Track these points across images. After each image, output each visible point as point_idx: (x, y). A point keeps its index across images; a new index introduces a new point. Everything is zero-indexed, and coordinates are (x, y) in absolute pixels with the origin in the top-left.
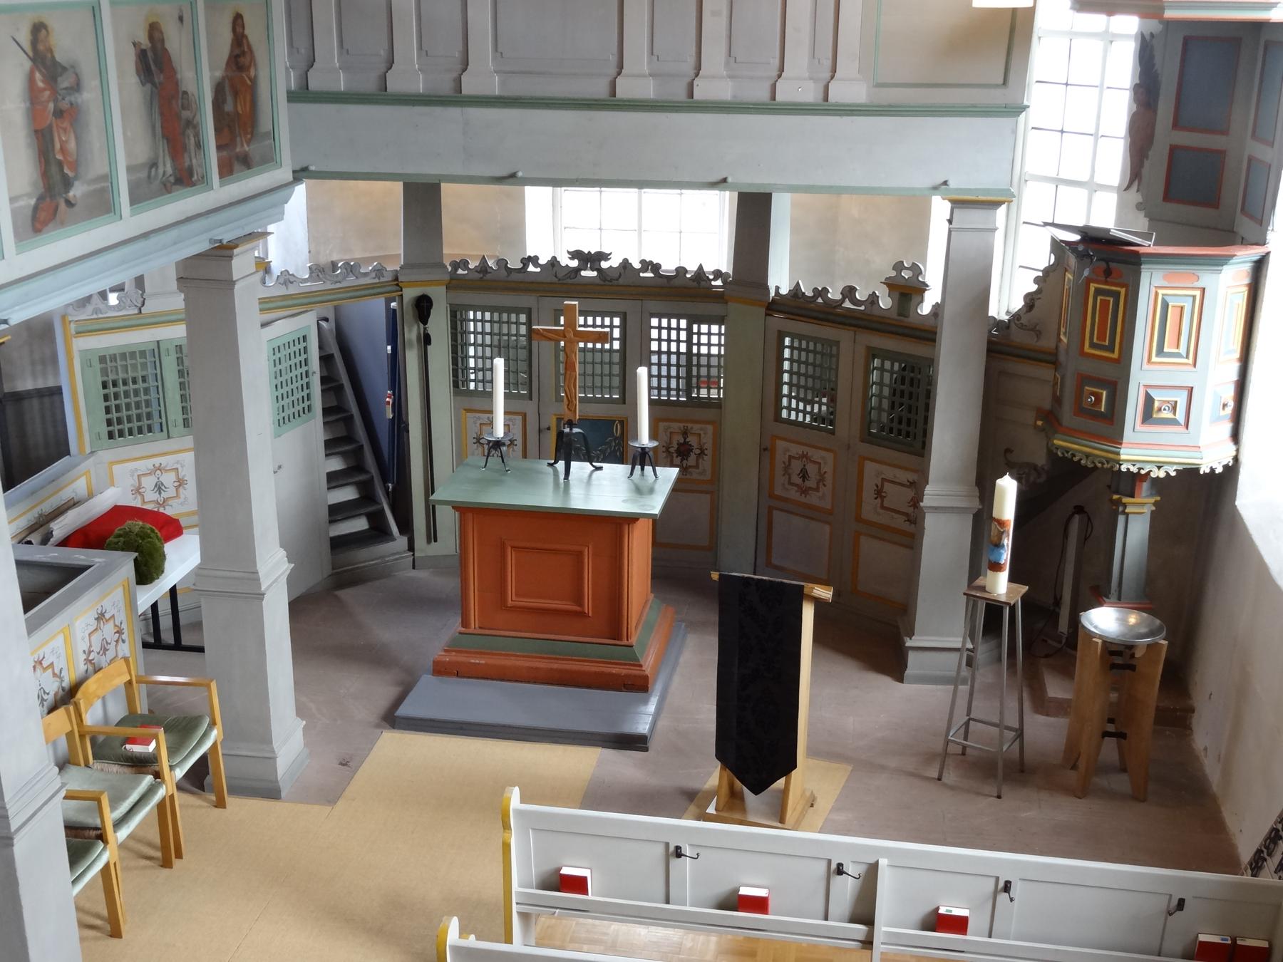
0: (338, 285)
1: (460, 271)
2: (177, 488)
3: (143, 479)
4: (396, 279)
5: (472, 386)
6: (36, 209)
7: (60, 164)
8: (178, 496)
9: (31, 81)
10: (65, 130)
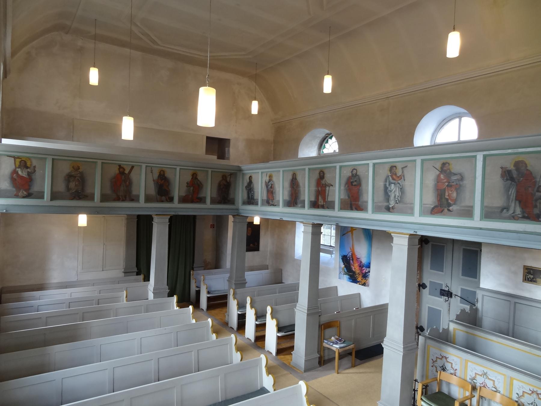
6: (433, 208)
7: (447, 200)
9: (439, 176)
10: (452, 191)
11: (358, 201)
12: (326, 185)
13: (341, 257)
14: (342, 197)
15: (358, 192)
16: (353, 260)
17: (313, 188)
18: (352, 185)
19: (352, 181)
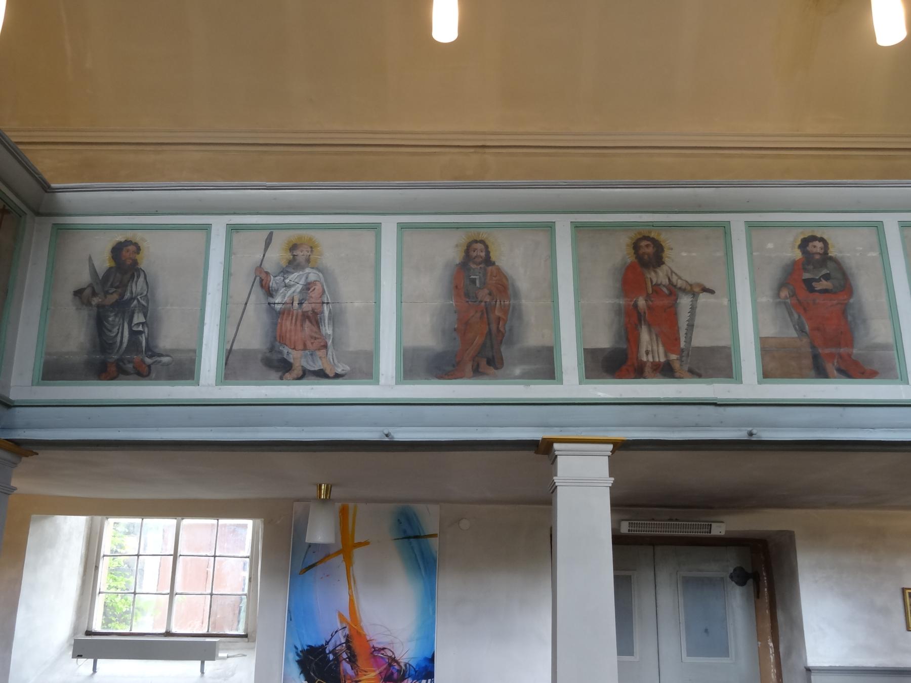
11: (850, 343)
12: (674, 291)
13: (293, 657)
14: (770, 331)
15: (844, 313)
16: (352, 659)
17: (605, 297)
18: (812, 290)
19: (806, 276)
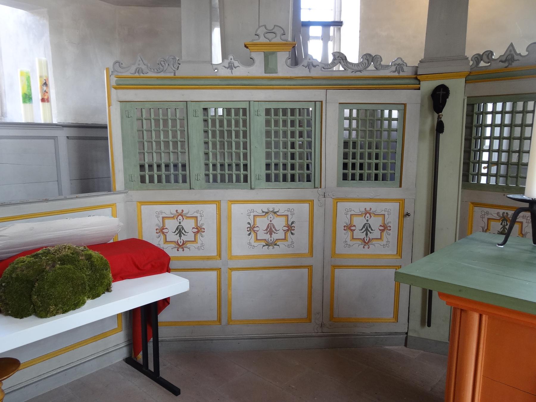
0: (358, 74)
1: (482, 64)
2: (196, 234)
3: (167, 221)
4: (416, 74)
5: (483, 180)
8: (195, 241)
